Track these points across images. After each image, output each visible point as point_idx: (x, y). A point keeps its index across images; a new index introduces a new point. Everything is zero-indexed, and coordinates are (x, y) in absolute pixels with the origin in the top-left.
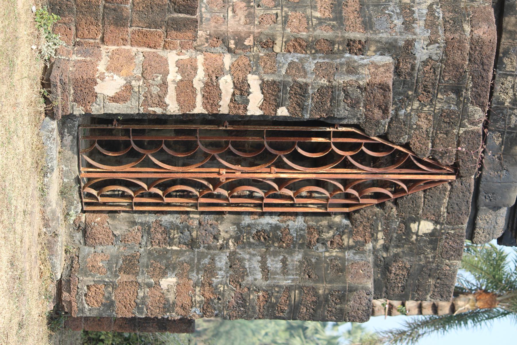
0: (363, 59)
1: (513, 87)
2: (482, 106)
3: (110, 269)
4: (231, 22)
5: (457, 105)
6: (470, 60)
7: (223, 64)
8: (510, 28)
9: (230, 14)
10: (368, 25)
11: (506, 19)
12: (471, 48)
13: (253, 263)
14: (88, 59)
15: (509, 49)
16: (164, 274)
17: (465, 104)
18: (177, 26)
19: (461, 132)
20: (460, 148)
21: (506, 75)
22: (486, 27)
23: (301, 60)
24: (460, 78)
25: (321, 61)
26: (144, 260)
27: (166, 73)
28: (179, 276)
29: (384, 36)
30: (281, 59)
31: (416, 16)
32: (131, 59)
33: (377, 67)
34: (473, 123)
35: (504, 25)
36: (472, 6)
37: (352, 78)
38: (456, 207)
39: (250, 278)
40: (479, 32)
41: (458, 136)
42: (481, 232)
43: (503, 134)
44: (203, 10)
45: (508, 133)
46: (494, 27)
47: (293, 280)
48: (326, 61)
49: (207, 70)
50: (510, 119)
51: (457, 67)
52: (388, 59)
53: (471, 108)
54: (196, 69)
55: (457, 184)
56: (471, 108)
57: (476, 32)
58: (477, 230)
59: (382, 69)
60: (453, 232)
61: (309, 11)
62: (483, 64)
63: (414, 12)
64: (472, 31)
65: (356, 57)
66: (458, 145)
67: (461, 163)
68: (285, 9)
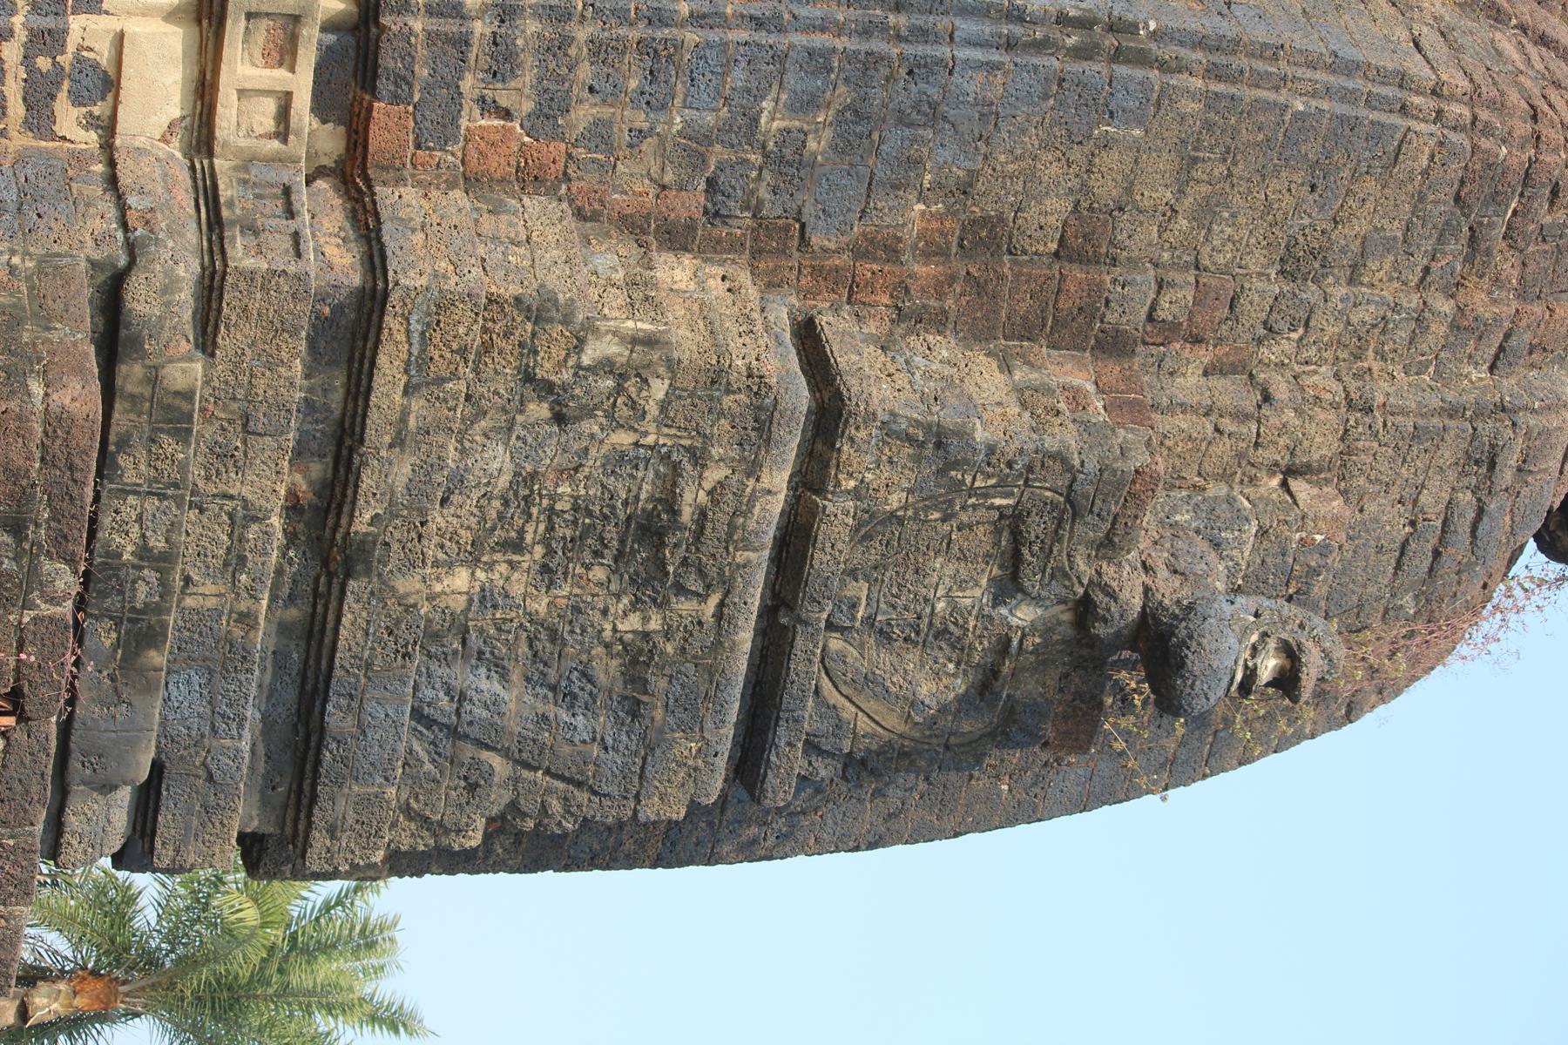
1: (139, 519)
2: (71, 561)
5: (17, 558)
6: (43, 459)
8: (131, 388)
11: (123, 369)
12: (46, 433)
15: (129, 435)
17: (33, 557)
19: (26, 620)
20: (23, 656)
21: (124, 493)
22: (79, 387)
24: (23, 498)
34: (52, 601)
35: (119, 382)
36: (46, 341)
38: (18, 788)
40: (62, 398)
41: (20, 628)
42: (74, 842)
43: (118, 623)
45: (130, 620)
46: (96, 387)
50: (134, 590)
51: (14, 475)
53: (47, 566)
55: (19, 736)
56: (47, 566)
57: (55, 396)
58: (67, 837)
60: (11, 842)
62: (71, 468)
64: (47, 394)
66: (20, 649)
67: (26, 690)
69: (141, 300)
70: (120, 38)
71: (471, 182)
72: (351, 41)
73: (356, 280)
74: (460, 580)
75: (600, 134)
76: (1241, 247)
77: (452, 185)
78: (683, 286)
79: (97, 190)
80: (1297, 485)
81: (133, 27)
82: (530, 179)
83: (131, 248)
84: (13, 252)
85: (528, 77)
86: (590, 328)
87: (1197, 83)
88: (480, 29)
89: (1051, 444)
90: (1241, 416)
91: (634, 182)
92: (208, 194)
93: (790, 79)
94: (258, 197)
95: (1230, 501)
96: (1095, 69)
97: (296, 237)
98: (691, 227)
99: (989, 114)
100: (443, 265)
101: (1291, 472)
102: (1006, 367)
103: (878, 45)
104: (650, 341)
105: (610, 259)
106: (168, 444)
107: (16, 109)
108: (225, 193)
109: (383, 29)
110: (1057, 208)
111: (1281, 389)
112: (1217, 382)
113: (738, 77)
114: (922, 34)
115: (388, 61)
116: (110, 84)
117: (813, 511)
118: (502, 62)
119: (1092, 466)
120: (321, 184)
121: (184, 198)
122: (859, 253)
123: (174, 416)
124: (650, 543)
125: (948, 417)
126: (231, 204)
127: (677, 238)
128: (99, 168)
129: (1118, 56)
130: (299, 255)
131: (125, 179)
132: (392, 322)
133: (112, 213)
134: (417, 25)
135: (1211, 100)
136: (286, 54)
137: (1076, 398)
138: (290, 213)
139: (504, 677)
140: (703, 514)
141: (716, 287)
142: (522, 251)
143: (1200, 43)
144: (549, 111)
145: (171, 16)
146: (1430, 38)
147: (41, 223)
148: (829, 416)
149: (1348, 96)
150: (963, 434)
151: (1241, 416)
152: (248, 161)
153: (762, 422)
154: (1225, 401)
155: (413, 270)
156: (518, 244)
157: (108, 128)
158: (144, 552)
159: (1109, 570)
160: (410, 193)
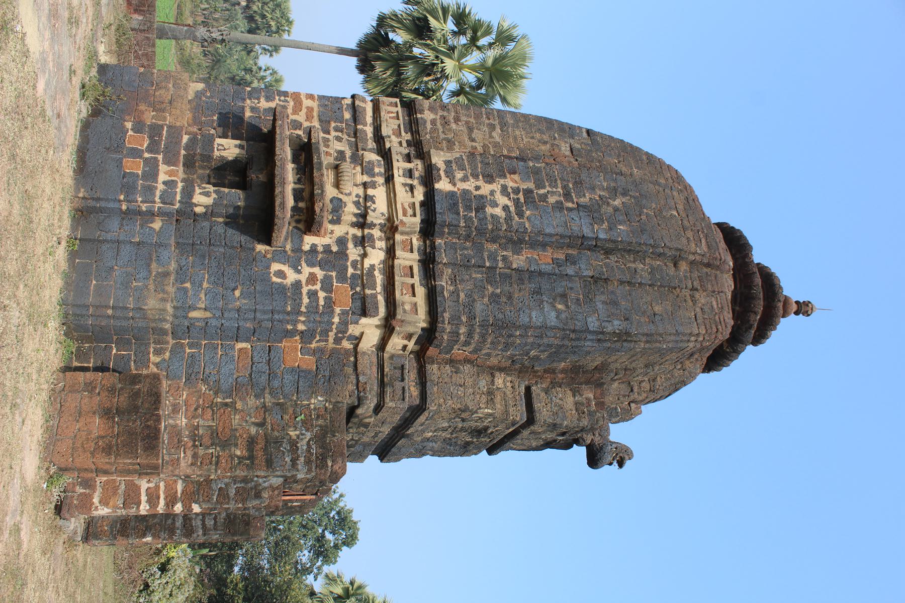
0: (265, 482)
3: (112, 532)
4: (183, 464)
7: (176, 492)
9: (182, 455)
10: (269, 464)
13: (197, 523)
14: (88, 491)
16: (144, 536)
18: (147, 474)
23: (226, 485)
25: (239, 485)
26: (133, 524)
27: (139, 503)
28: (154, 536)
29: (278, 473)
30: (214, 486)
31: (299, 452)
32: (116, 489)
33: (273, 489)
36: (334, 442)
37: (257, 502)
39: (195, 535)
44: (165, 451)
47: (220, 535)
48: (242, 485)
49: (165, 499)
52: (282, 479)
54: (159, 498)
59: (276, 492)
61: (233, 449)
63: (297, 448)
65: (261, 480)
68: (218, 448)
69: (359, 411)
70: (363, 333)
71: (451, 362)
72: (426, 334)
73: (417, 402)
74: (431, 434)
75: (489, 355)
76: (640, 364)
77: (446, 364)
78: (500, 386)
79: (349, 370)
80: (633, 405)
81: (367, 331)
82: (467, 361)
83: (359, 399)
84: (326, 401)
85: (473, 346)
86: (476, 412)
87: (642, 345)
88: (462, 338)
89: (581, 425)
90: (624, 396)
91: (494, 361)
92: (381, 367)
93: (541, 348)
94: (395, 368)
95: (616, 408)
96: (618, 344)
97: (403, 388)
98: (505, 368)
99: (589, 353)
100: (442, 400)
101: (632, 402)
102: (574, 396)
103: (566, 342)
104: (491, 415)
105: (483, 384)
106: (362, 428)
107: (331, 340)
108: (386, 370)
109: (436, 337)
110: (596, 364)
111: (636, 389)
112: (623, 386)
113: (528, 347)
114: (578, 339)
115: (435, 342)
116: (359, 339)
117: (520, 432)
118: (467, 343)
119: (589, 427)
120: (412, 356)
121: (375, 369)
122: (545, 371)
123: (366, 426)
124: (479, 432)
125: (558, 421)
126: (387, 375)
127: (501, 370)
128: (352, 359)
129: (625, 341)
130: (403, 400)
131: (359, 369)
132: (426, 413)
133: (355, 381)
134: (446, 337)
135: (644, 349)
136: (409, 337)
137: (588, 399)
138: (403, 380)
139: (436, 442)
140: (492, 433)
141: (508, 384)
142: (462, 389)
143: (647, 335)
144: (475, 351)
145: (377, 326)
146: (699, 315)
147: (335, 387)
148: (531, 420)
149: (677, 342)
150: (561, 424)
151: (624, 396)
152: (392, 357)
153: (513, 425)
154: (622, 393)
155: (433, 408)
156: (461, 386)
157: (356, 346)
158: (352, 439)
159: (585, 436)
160: (435, 366)
